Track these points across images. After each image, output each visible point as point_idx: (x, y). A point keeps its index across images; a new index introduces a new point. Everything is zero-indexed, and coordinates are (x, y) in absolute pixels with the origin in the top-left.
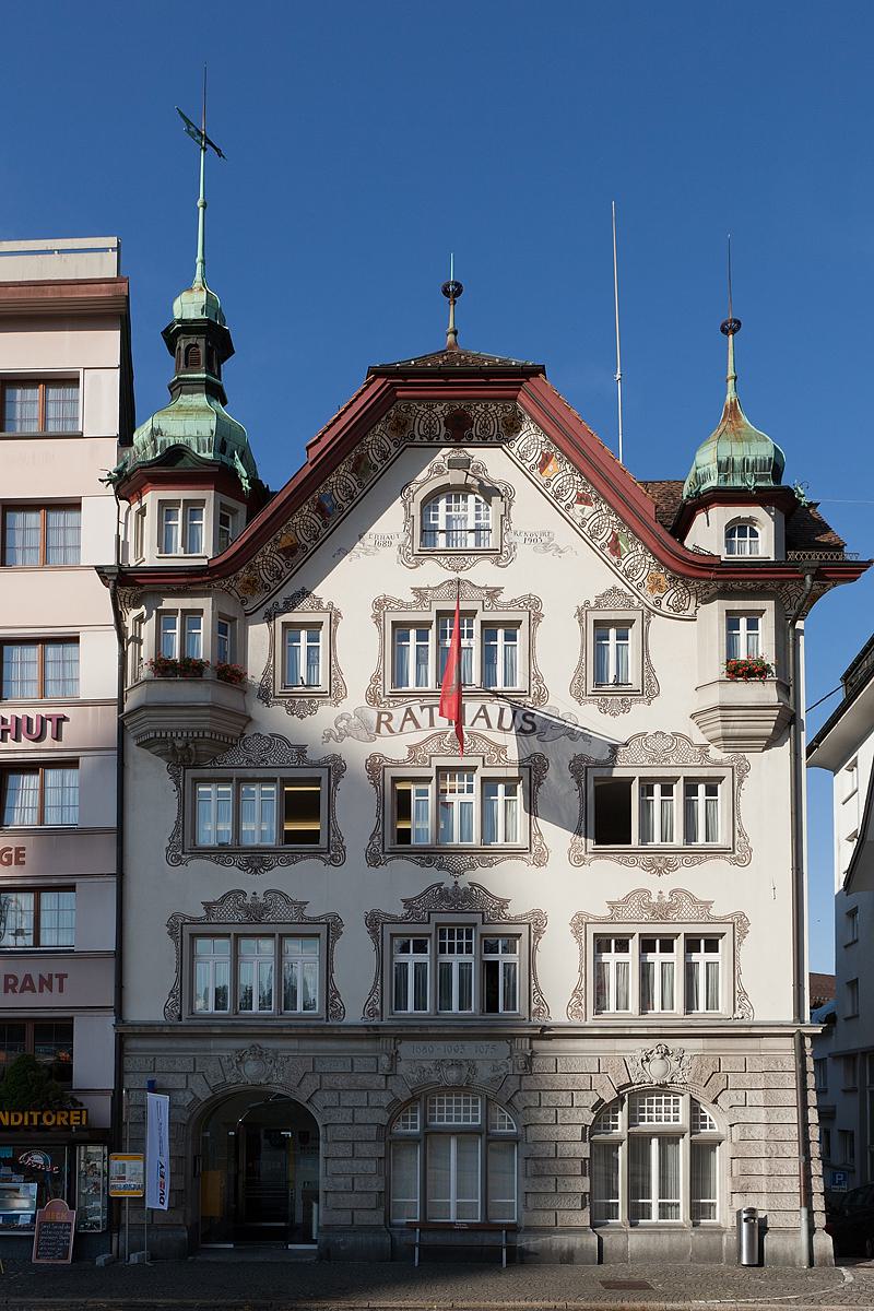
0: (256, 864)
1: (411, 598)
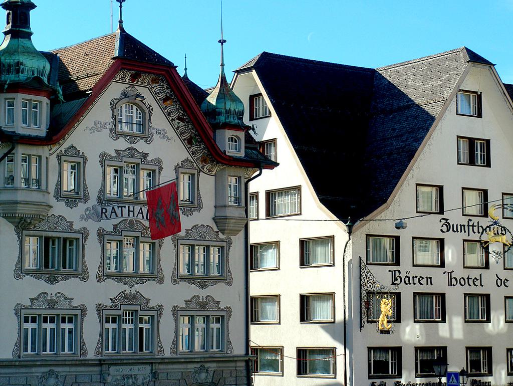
0: (52, 280)
1: (114, 154)
